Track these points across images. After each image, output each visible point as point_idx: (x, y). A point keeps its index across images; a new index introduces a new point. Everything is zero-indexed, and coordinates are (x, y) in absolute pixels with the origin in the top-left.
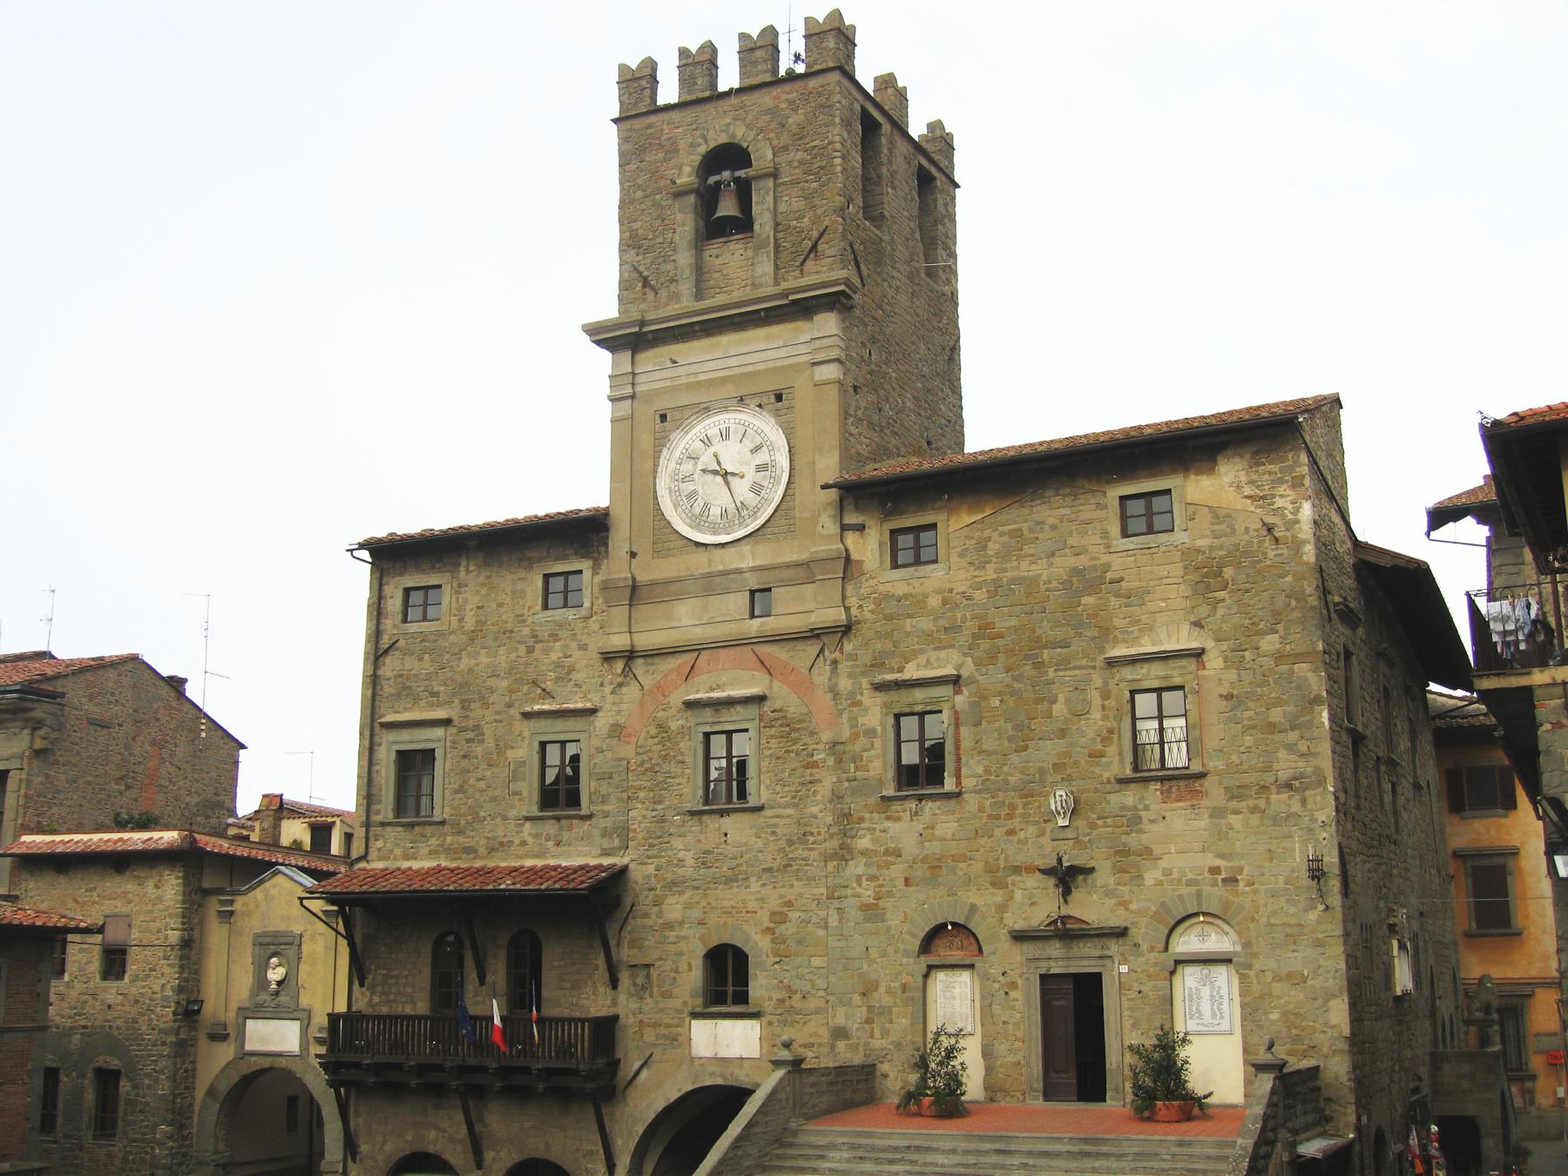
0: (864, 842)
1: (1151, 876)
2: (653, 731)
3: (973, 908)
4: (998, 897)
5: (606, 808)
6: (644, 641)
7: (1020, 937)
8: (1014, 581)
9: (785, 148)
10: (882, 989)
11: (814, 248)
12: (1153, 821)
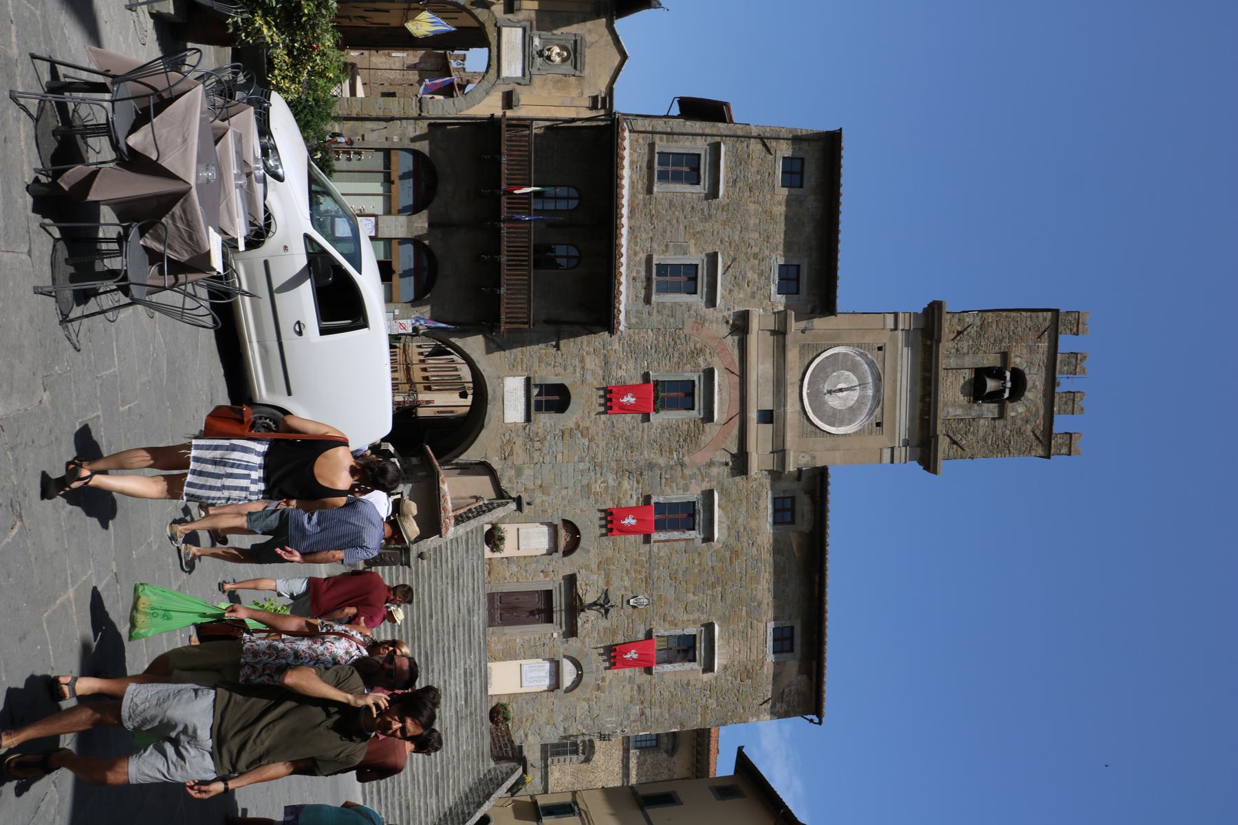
0: (626, 485)
2: (698, 346)
3: (588, 551)
4: (594, 566)
6: (753, 339)
7: (571, 580)
8: (759, 573)
9: (1014, 423)
10: (545, 498)
11: (955, 442)
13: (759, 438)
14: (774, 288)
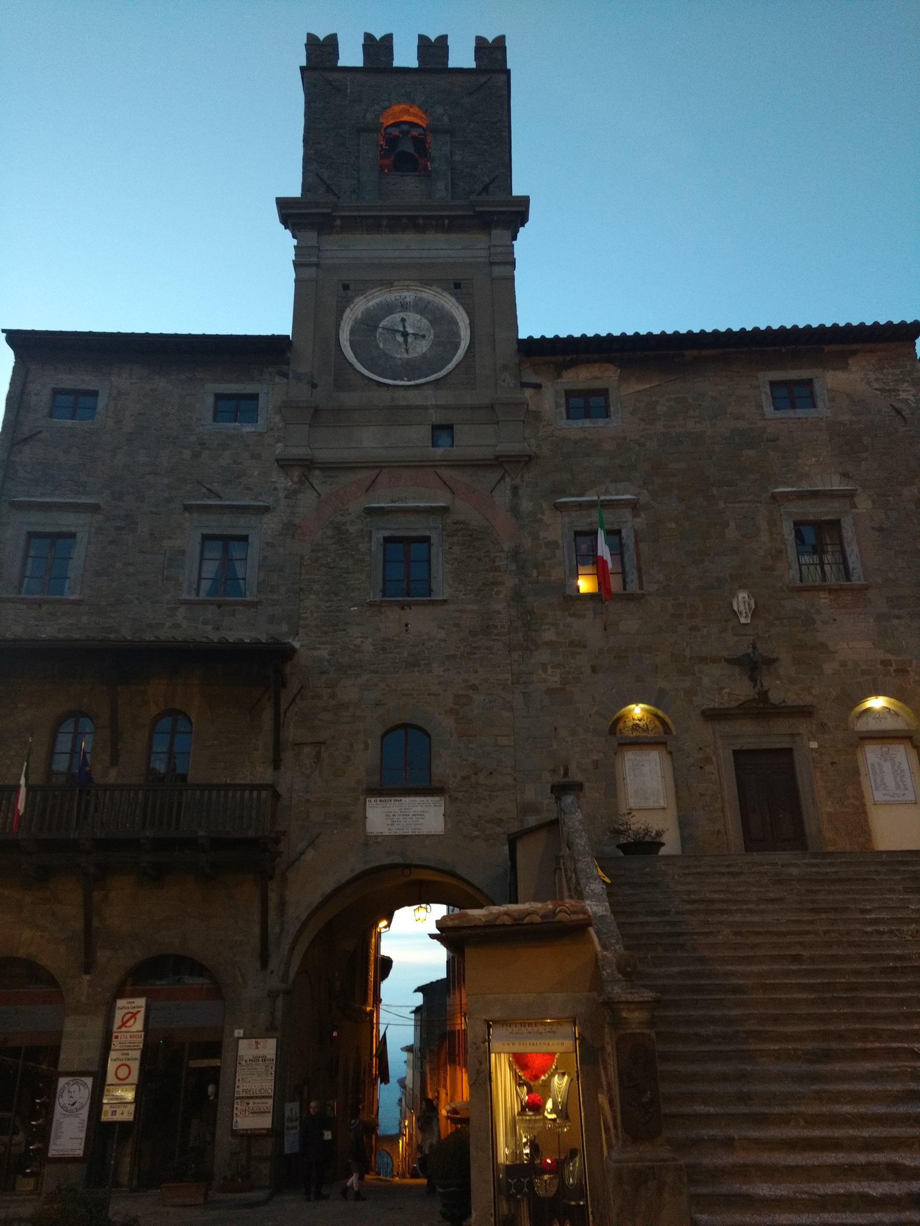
1: (829, 668)
2: (330, 533)
5: (275, 597)
6: (324, 455)
7: (712, 716)
11: (486, 189)
12: (825, 623)
13: (473, 441)
14: (248, 429)
